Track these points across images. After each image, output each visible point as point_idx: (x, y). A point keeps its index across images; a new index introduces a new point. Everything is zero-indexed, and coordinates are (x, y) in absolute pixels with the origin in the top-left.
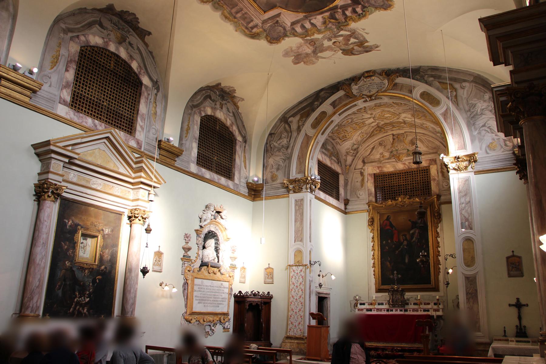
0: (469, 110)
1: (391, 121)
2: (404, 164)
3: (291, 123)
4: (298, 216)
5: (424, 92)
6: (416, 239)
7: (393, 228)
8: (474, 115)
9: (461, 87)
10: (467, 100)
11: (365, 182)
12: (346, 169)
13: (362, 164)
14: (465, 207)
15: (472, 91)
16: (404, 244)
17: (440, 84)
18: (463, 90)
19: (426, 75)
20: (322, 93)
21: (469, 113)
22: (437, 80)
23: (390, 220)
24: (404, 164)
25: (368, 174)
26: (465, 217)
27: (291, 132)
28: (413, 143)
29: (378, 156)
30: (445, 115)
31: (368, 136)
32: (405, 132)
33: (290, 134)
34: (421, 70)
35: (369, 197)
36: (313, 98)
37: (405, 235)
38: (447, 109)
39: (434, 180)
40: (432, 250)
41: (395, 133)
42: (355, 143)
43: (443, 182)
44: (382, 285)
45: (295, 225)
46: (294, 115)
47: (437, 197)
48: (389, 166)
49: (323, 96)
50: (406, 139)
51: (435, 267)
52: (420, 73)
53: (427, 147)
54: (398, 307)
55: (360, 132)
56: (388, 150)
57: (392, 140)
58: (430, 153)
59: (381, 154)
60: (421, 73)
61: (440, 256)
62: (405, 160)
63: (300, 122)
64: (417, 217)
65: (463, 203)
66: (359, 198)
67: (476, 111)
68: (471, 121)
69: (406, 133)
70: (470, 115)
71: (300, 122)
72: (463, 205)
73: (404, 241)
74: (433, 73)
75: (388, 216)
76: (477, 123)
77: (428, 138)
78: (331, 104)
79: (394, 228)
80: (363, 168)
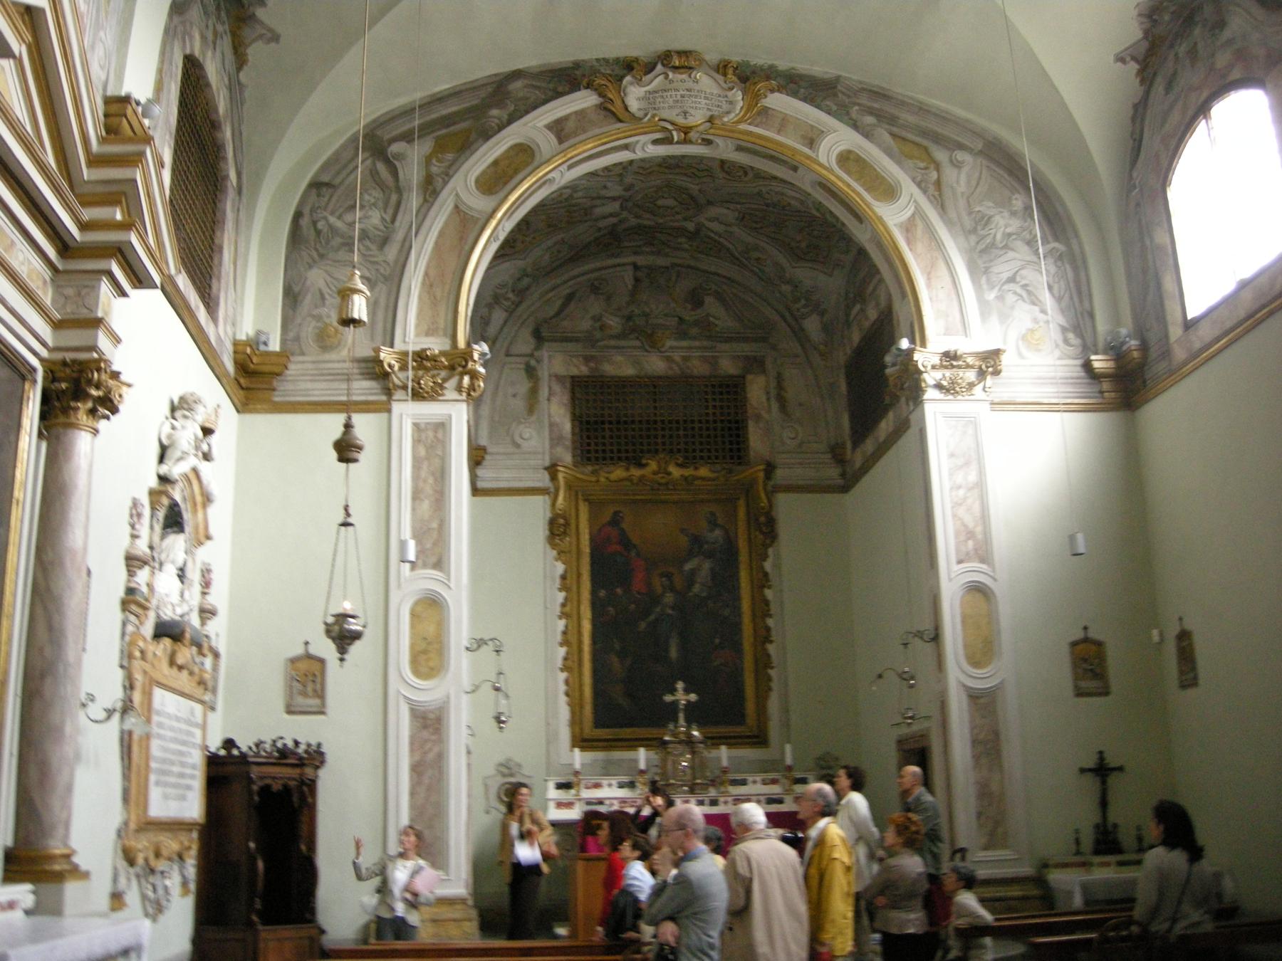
0: (974, 231)
1: (661, 221)
2: (669, 359)
3: (397, 160)
4: (425, 481)
5: (849, 152)
8: (987, 247)
9: (951, 161)
10: (968, 202)
11: (541, 399)
13: (532, 341)
14: (965, 498)
15: (980, 178)
17: (894, 139)
18: (955, 171)
19: (855, 104)
20: (518, 85)
21: (973, 239)
22: (887, 127)
25: (550, 376)
26: (965, 526)
27: (399, 190)
28: (695, 299)
29: (586, 325)
30: (908, 230)
33: (394, 197)
34: (839, 87)
35: (552, 447)
36: (483, 94)
37: (669, 576)
38: (913, 215)
41: (640, 260)
42: (529, 270)
44: (596, 727)
45: (414, 509)
46: (407, 137)
47: (765, 470)
48: (619, 358)
49: (521, 94)
52: (835, 95)
54: (692, 791)
55: (560, 237)
56: (619, 309)
57: (632, 282)
58: (746, 340)
59: (596, 319)
60: (840, 95)
61: (771, 642)
62: (671, 348)
63: (434, 161)
65: (959, 487)
66: (518, 446)
67: (991, 236)
68: (980, 262)
70: (978, 243)
71: (434, 161)
72: (961, 492)
74: (876, 105)
75: (616, 513)
76: (995, 270)
78: (549, 127)
80: (536, 354)
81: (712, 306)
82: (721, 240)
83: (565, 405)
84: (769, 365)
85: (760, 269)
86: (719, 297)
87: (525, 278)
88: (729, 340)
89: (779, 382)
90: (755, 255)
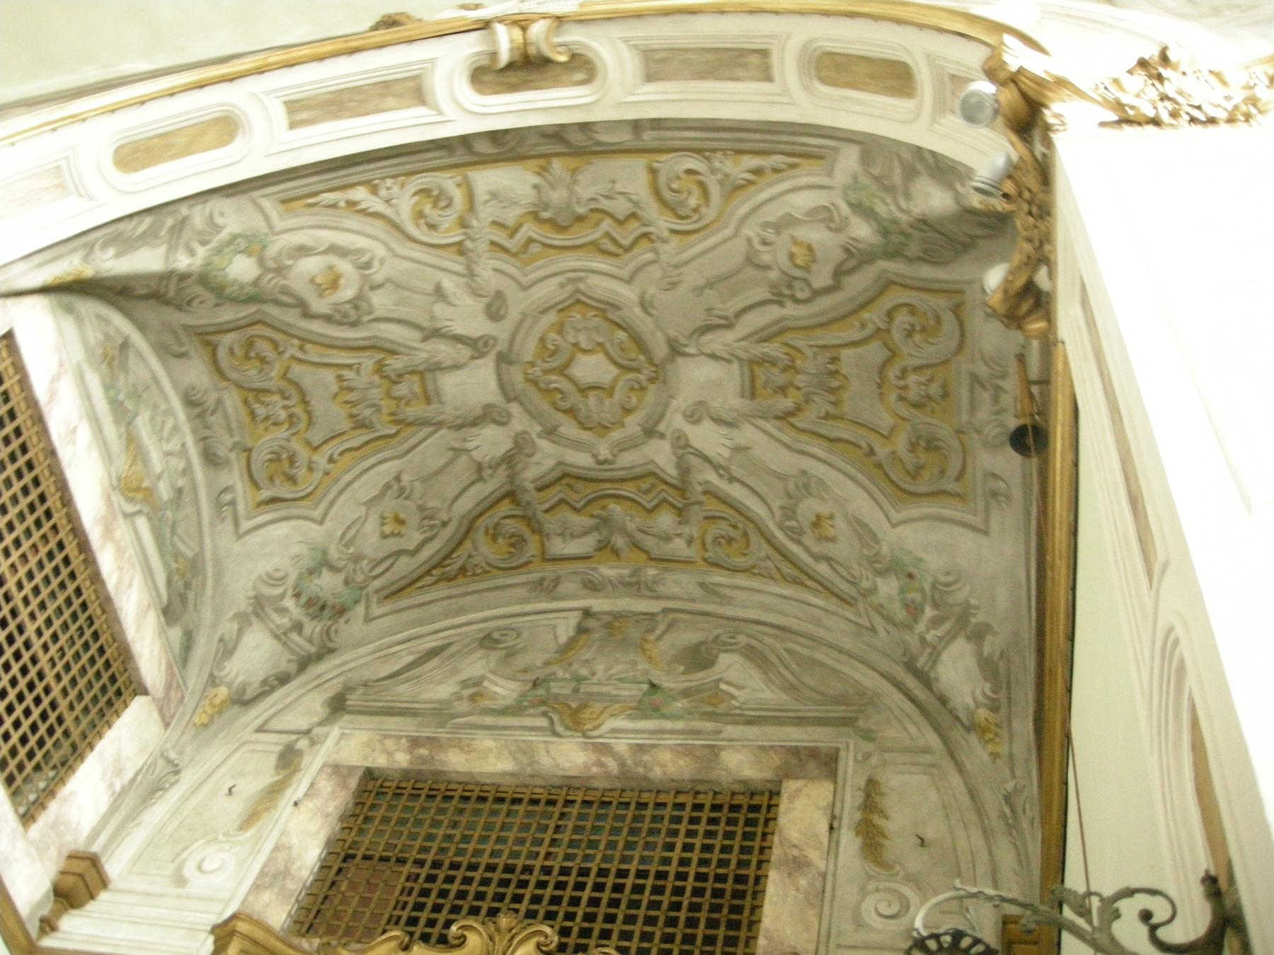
12: (203, 696)
24: (604, 749)
28: (698, 658)
31: (427, 552)
32: (666, 611)
35: (257, 888)
39: (798, 864)
42: (334, 554)
43: (863, 892)
48: (489, 743)
50: (659, 638)
53: (790, 688)
55: (389, 468)
57: (571, 633)
58: (800, 721)
62: (614, 731)
66: (180, 880)
69: (672, 616)
77: (805, 652)
80: (317, 731)
81: (730, 667)
82: (736, 492)
83: (327, 816)
84: (848, 764)
85: (829, 559)
86: (753, 655)
87: (325, 572)
88: (750, 722)
89: (868, 795)
90: (810, 507)
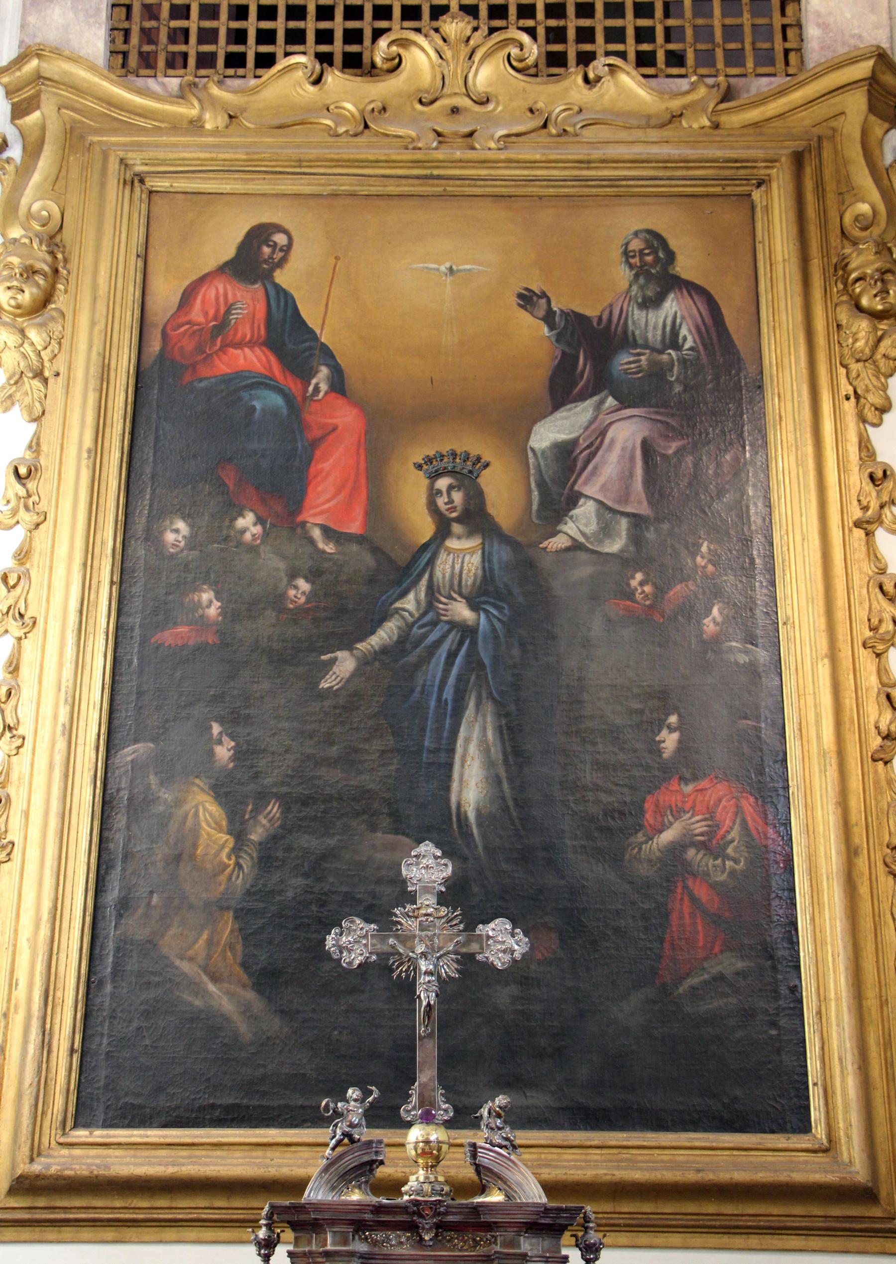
6: (606, 531)
7: (305, 374)
16: (444, 567)
23: (282, 277)
40: (824, 670)
51: (864, 890)
64: (623, 275)
73: (443, 530)
79: (324, 371)
